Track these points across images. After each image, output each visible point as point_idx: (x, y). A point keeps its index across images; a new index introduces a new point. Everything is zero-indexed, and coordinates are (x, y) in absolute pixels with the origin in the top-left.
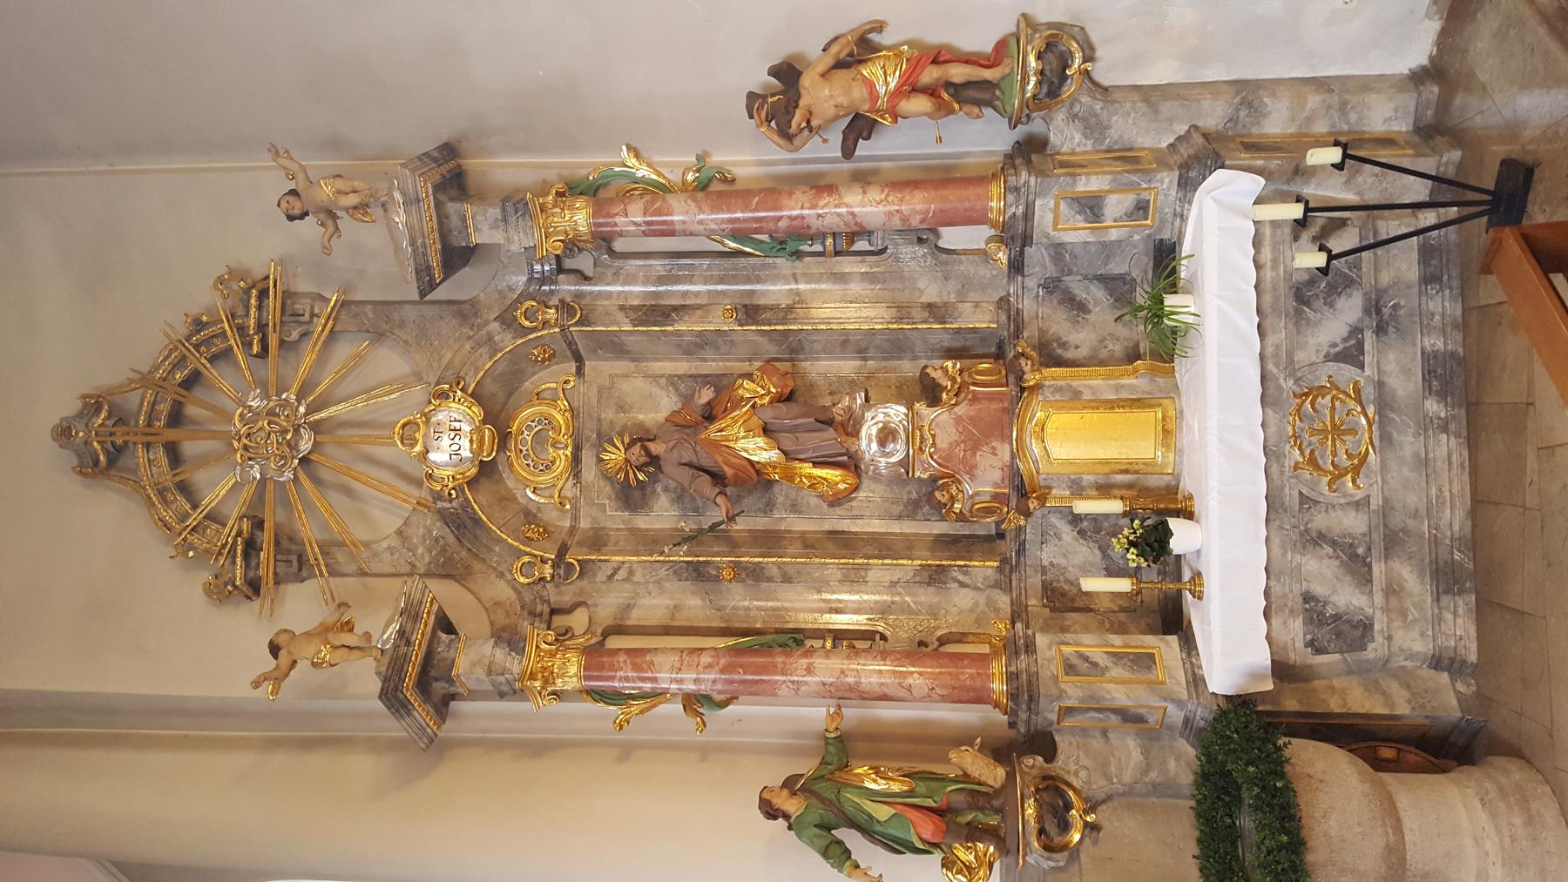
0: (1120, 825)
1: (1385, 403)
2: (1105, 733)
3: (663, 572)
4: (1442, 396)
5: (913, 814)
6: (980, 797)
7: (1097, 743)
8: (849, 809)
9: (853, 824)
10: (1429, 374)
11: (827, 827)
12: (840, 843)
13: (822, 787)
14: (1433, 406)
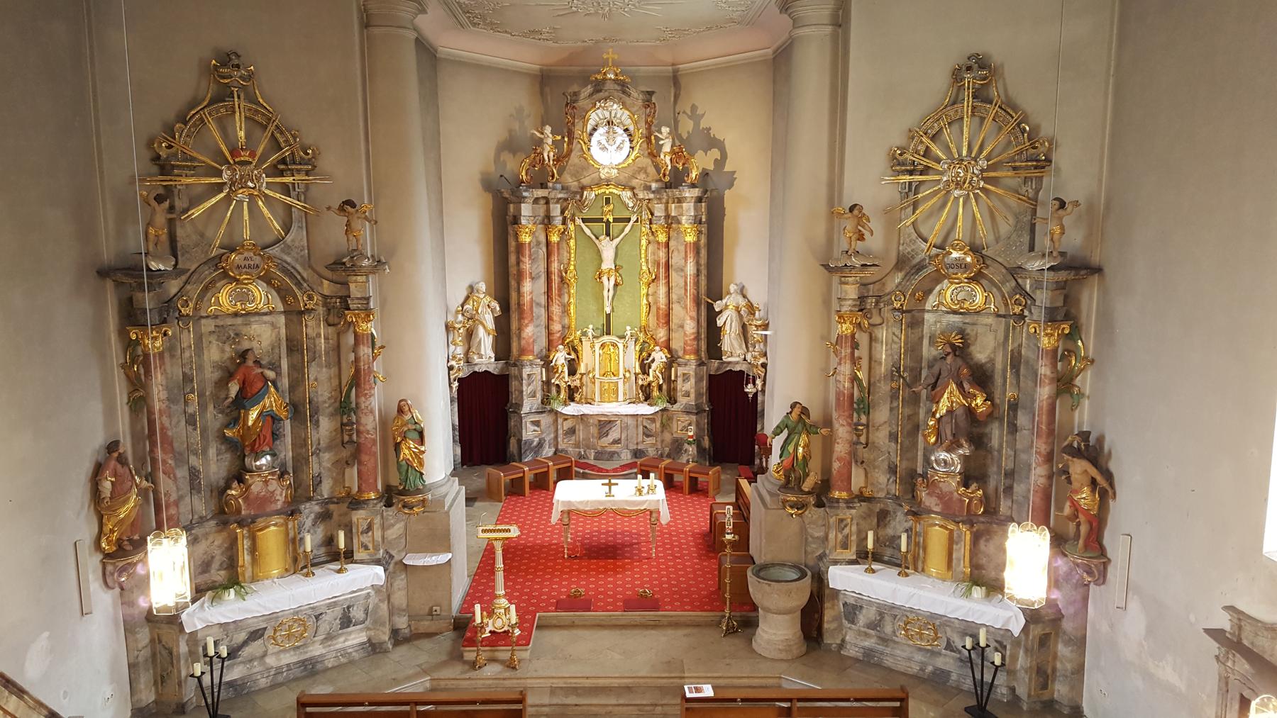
0: (793, 526)
1: (934, 654)
2: (824, 525)
3: (896, 357)
4: (933, 673)
6: (800, 481)
7: (820, 522)
8: (792, 436)
9: (789, 435)
10: (943, 671)
12: (782, 432)
14: (930, 668)
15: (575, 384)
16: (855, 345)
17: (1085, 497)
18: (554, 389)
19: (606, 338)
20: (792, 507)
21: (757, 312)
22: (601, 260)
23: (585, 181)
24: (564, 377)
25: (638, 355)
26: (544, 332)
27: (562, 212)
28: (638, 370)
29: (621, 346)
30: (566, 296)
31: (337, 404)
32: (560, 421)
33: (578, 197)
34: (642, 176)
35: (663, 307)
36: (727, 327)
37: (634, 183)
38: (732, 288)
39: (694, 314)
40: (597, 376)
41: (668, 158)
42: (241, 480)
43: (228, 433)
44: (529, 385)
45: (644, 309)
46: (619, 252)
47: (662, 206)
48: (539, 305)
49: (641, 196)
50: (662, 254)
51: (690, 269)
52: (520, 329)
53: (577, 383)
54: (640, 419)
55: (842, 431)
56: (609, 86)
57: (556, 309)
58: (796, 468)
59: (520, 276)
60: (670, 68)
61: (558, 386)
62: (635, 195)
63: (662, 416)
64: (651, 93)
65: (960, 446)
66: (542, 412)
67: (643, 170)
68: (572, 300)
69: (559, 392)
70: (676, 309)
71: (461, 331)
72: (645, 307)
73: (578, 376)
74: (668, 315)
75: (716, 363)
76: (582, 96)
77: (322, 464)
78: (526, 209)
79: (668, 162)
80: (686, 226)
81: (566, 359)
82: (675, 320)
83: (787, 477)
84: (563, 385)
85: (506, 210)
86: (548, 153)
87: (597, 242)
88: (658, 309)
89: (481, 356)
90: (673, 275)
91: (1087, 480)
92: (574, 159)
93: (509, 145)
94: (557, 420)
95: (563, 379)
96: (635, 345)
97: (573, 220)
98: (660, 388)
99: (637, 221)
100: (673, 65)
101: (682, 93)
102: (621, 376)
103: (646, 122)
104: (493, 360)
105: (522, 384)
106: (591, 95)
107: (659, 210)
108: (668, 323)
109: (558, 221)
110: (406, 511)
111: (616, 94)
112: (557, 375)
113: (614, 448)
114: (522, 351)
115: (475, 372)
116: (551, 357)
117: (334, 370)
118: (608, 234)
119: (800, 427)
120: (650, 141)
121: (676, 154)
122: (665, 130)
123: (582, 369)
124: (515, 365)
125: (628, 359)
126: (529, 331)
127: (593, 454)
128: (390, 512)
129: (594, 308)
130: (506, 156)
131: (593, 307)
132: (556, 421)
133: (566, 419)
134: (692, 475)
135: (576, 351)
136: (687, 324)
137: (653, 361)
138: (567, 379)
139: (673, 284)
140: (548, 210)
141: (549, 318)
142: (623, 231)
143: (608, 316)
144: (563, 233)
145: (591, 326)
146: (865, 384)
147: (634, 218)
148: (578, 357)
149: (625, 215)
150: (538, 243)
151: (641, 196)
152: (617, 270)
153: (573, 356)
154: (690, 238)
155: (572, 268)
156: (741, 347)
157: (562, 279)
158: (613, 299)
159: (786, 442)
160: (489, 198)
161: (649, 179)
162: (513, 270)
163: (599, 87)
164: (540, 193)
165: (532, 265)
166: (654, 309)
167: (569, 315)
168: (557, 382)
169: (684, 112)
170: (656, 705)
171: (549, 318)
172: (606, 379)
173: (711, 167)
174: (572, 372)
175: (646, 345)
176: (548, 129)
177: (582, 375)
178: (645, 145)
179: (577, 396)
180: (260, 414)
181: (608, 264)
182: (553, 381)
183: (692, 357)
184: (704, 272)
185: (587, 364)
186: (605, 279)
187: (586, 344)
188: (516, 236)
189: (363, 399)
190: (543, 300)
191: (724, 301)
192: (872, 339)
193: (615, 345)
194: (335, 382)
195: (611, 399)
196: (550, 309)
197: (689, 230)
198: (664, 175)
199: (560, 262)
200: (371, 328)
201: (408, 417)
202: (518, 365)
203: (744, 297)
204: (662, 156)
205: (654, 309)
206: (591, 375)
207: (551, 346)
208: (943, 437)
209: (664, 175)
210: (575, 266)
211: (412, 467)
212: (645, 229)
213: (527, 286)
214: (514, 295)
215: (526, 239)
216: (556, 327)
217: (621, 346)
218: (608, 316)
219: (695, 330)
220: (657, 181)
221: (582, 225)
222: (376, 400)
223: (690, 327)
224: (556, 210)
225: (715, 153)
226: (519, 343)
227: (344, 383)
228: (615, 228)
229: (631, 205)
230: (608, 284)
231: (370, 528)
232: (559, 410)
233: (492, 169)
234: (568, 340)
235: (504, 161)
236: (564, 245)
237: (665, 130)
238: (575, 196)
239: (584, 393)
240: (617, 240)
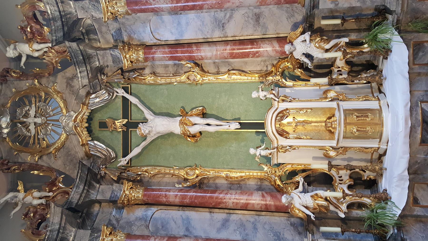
15: (346, 178)
24: (335, 198)
25: (300, 83)
26: (266, 218)
32: (418, 211)
40: (334, 143)
41: (36, 46)
45: (236, 78)
46: (164, 111)
48: (225, 223)
54: (417, 69)
61: (350, 206)
63: (407, 32)
69: (361, 206)
72: (234, 77)
73: (333, 172)
81: (305, 191)
88: (233, 56)
94: (417, 216)
96: (285, 87)
99: (126, 90)
102: (334, 104)
116: (301, 215)
118: (135, 125)
129: (234, 145)
131: (234, 146)
132: (418, 219)
133: (416, 201)
135: (293, 174)
137: (308, 56)
138: (339, 194)
143: (243, 126)
148: (304, 171)
153: (300, 179)
155: (182, 173)
167: (243, 179)
168: (344, 207)
172: (340, 130)
175: (286, 73)
177: (331, 166)
182: (343, 216)
185: (315, 158)
186: (193, 130)
187: (282, 158)
195: (377, 121)
206: (332, 153)
210: (180, 169)
218: (243, 126)
221: (128, 158)
232: (399, 212)
234: (278, 182)
239: (363, 164)
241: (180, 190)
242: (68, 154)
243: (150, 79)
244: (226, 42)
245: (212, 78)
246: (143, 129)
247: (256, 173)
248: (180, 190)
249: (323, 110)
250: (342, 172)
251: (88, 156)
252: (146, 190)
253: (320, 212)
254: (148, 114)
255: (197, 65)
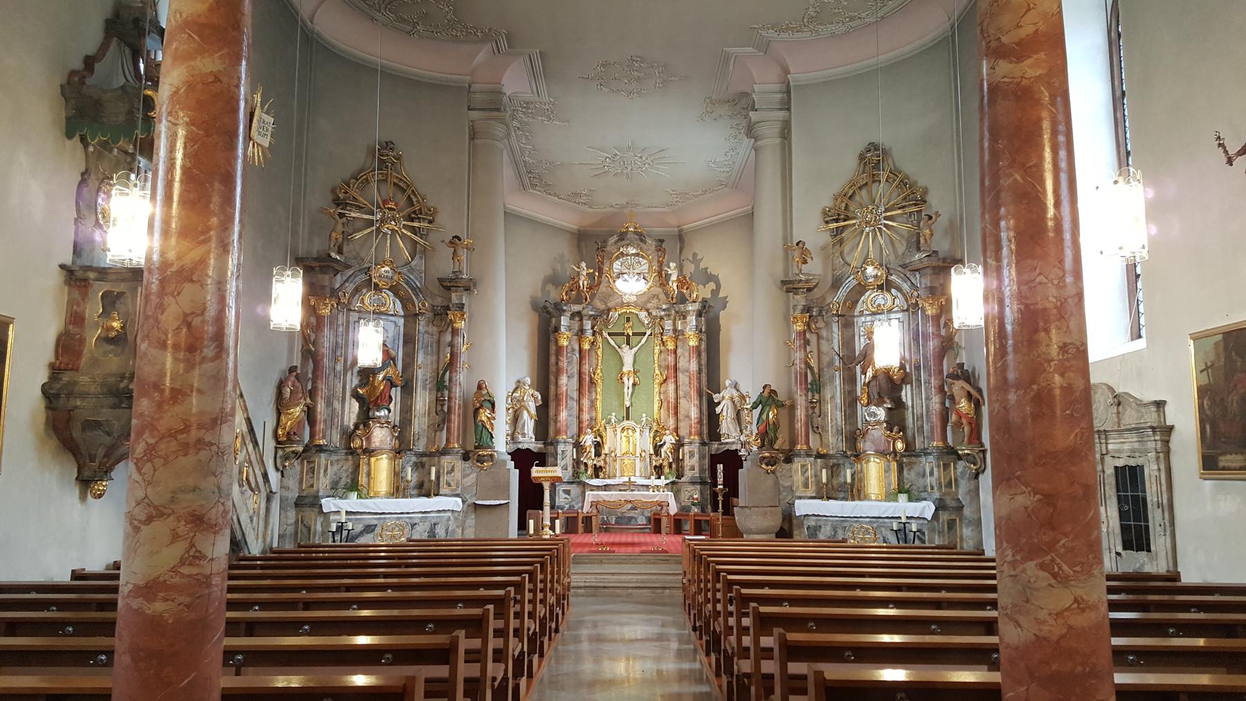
5: (764, 424)
6: (772, 443)
11: (760, 403)
13: (771, 400)
16: (807, 342)
17: (964, 405)
18: (583, 467)
19: (626, 423)
20: (767, 465)
21: (747, 399)
22: (622, 364)
23: (610, 305)
26: (575, 421)
27: (592, 328)
28: (652, 452)
29: (638, 430)
30: (594, 393)
31: (435, 382)
33: (605, 317)
34: (655, 301)
35: (672, 400)
36: (724, 413)
37: (649, 306)
38: (728, 383)
39: (697, 402)
41: (675, 285)
42: (366, 425)
43: (360, 391)
44: (563, 459)
45: (656, 405)
47: (670, 322)
49: (654, 314)
50: (671, 359)
51: (694, 366)
52: (556, 415)
53: (602, 463)
55: (801, 402)
56: (630, 236)
57: (586, 403)
58: (769, 432)
59: (558, 372)
60: (676, 229)
62: (650, 314)
64: (662, 241)
65: (885, 402)
66: (572, 483)
67: (656, 296)
68: (598, 397)
70: (682, 401)
71: (510, 411)
73: (603, 456)
74: (676, 408)
75: (715, 445)
76: (609, 243)
77: (420, 423)
78: (564, 321)
79: (675, 288)
80: (690, 333)
82: (682, 412)
83: (763, 441)
84: (590, 463)
85: (549, 322)
86: (583, 282)
87: (619, 350)
89: (524, 435)
90: (680, 376)
91: (965, 394)
92: (603, 288)
93: (553, 280)
95: (590, 459)
97: (601, 334)
98: (670, 466)
100: (678, 227)
101: (686, 245)
103: (659, 262)
104: (533, 440)
105: (556, 459)
106: (616, 242)
107: (668, 325)
108: (676, 414)
109: (589, 332)
110: (479, 464)
111: (635, 242)
112: (585, 454)
113: (632, 514)
114: (558, 432)
115: (519, 449)
117: (435, 358)
118: (628, 344)
119: (771, 400)
120: (661, 274)
121: (682, 282)
122: (673, 265)
123: (606, 450)
124: (552, 444)
125: (644, 442)
126: (563, 415)
127: (614, 519)
128: (468, 464)
130: (550, 287)
131: (616, 403)
134: (696, 518)
135: (601, 437)
136: (691, 409)
139: (680, 383)
140: (582, 325)
141: (580, 410)
142: (640, 342)
143: (628, 409)
144: (593, 343)
145: (614, 414)
146: (816, 370)
147: (649, 332)
149: (642, 330)
150: (573, 350)
151: (654, 314)
152: (635, 372)
153: (599, 439)
154: (693, 343)
155: (599, 371)
156: (736, 431)
157: (591, 379)
158: (632, 395)
159: (761, 414)
160: (535, 317)
161: (661, 303)
162: (553, 369)
163: (622, 237)
164: (576, 308)
165: (569, 364)
166: (665, 404)
169: (687, 259)
170: (666, 588)
171: (580, 410)
173: (709, 296)
174: (598, 454)
176: (583, 265)
177: (606, 454)
178: (657, 278)
179: (601, 474)
180: (383, 379)
181: (628, 367)
183: (696, 437)
184: (704, 370)
185: (610, 448)
186: (625, 379)
188: (557, 341)
189: (455, 374)
190: (575, 395)
191: (721, 394)
192: (819, 337)
193: (634, 430)
194: (435, 366)
196: (581, 402)
197: (692, 337)
198: (672, 298)
199: (590, 366)
200: (461, 325)
201: (484, 392)
202: (555, 443)
203: (738, 391)
204: (670, 284)
205: (665, 404)
206: (613, 455)
207: (580, 431)
208: (872, 397)
209: (672, 298)
211: (486, 427)
212: (658, 341)
213: (564, 380)
214: (552, 388)
215: (564, 342)
216: (585, 417)
217: (638, 430)
219: (698, 416)
220: (666, 304)
222: (463, 382)
223: (694, 413)
224: (588, 325)
225: (712, 285)
226: (556, 427)
227: (440, 368)
228: (634, 340)
229: (646, 322)
230: (628, 382)
231: (453, 470)
233: (540, 294)
235: (549, 291)
236: (593, 353)
237: (673, 265)
238: (601, 316)
240: (635, 349)
241: (589, 372)
242: (610, 296)
243: (657, 351)
244: (677, 398)
245: (657, 390)
246: (626, 348)
247: (600, 416)
248: (589, 372)
249: (635, 451)
250: (602, 462)
251: (609, 310)
252: (589, 350)
253: (582, 449)
254: (635, 349)
255: (665, 381)
